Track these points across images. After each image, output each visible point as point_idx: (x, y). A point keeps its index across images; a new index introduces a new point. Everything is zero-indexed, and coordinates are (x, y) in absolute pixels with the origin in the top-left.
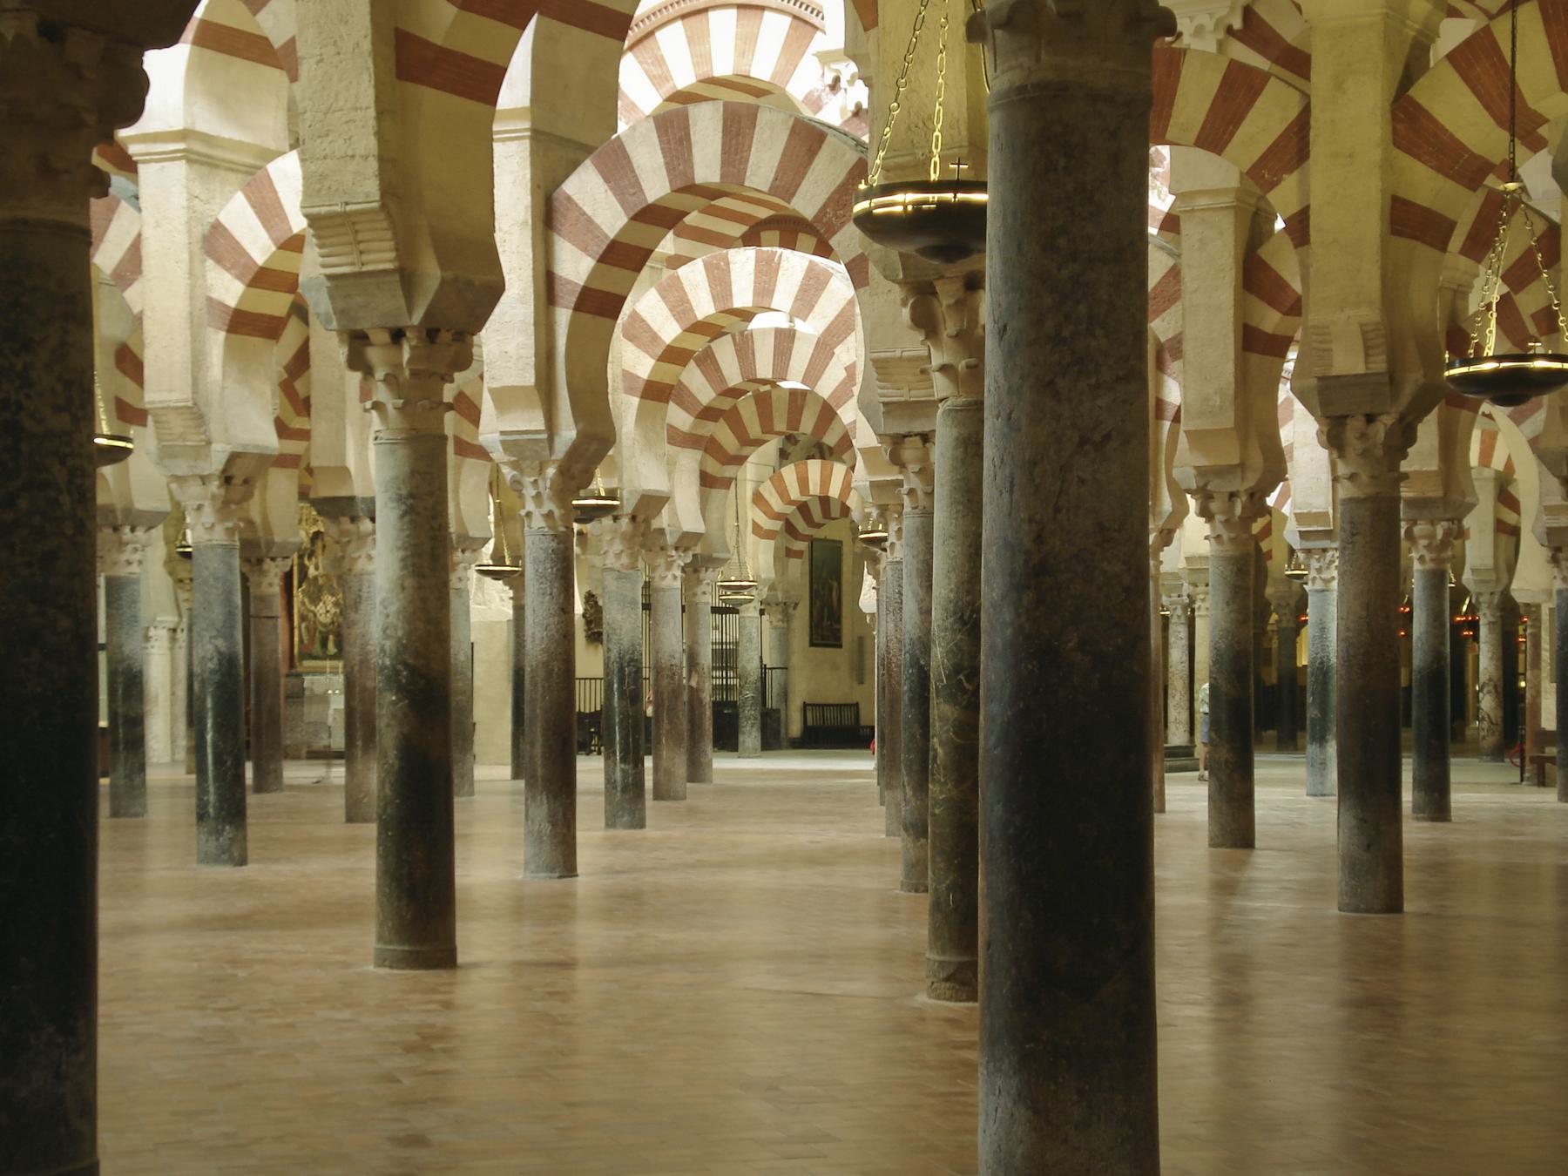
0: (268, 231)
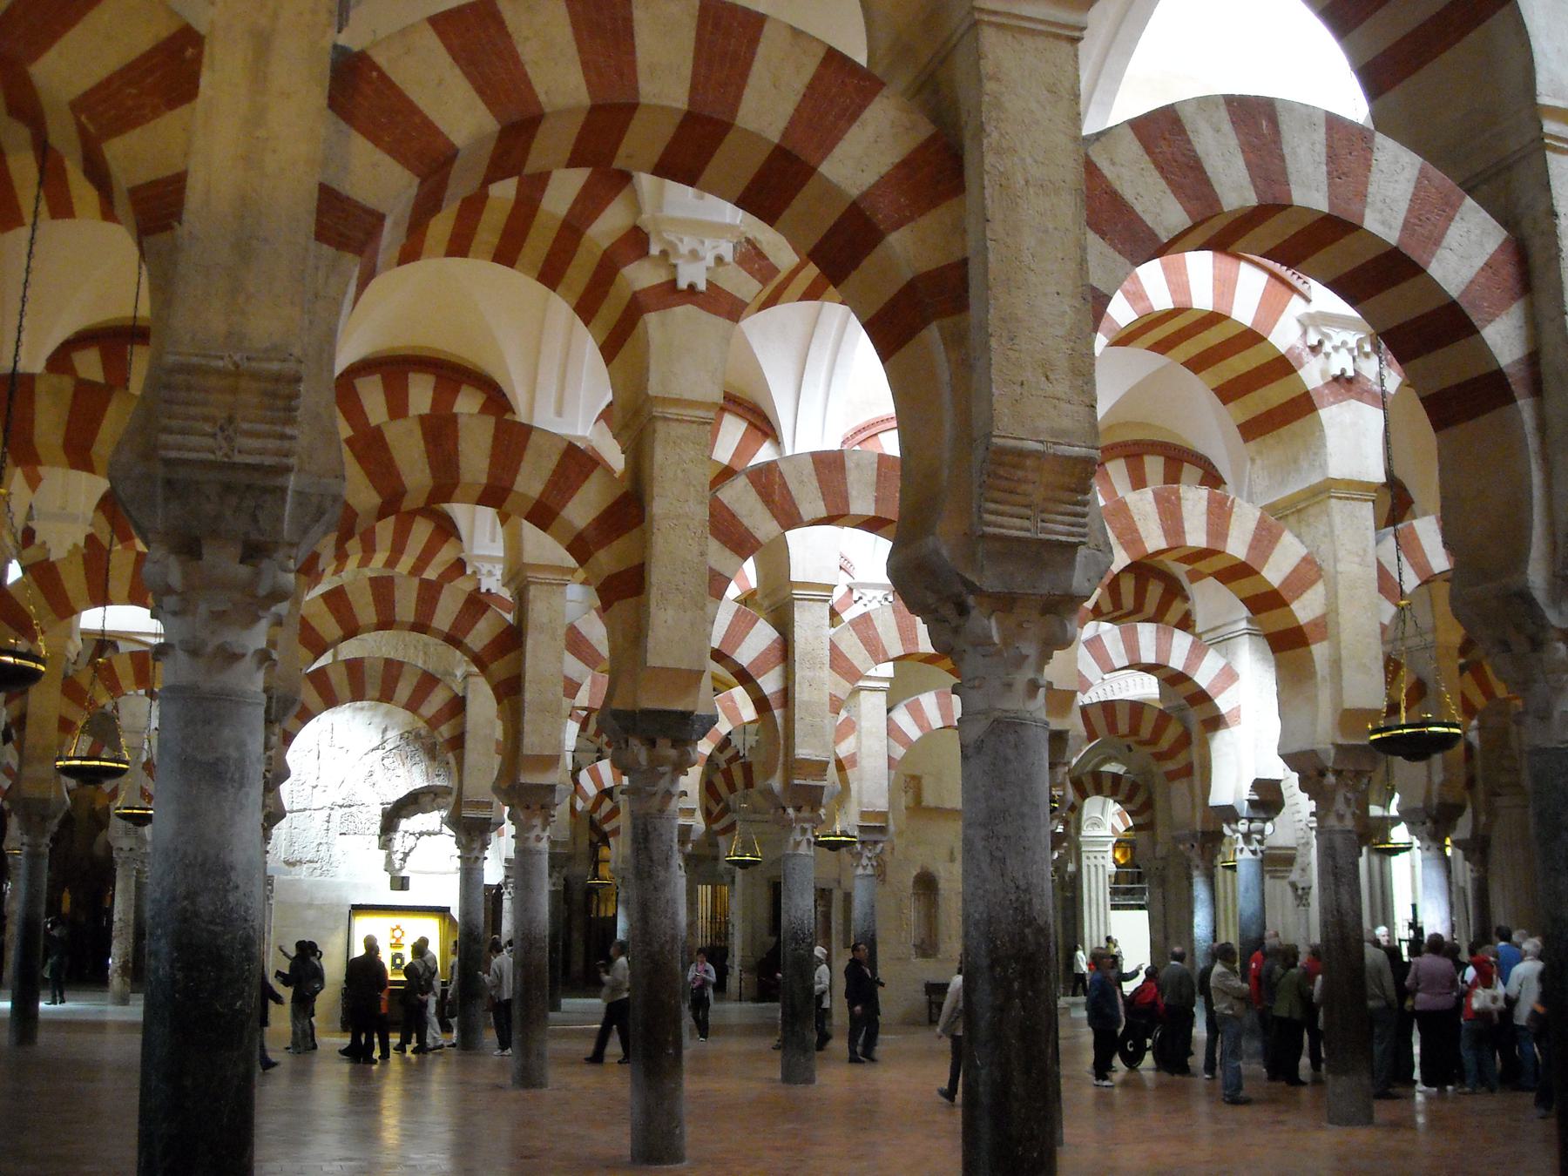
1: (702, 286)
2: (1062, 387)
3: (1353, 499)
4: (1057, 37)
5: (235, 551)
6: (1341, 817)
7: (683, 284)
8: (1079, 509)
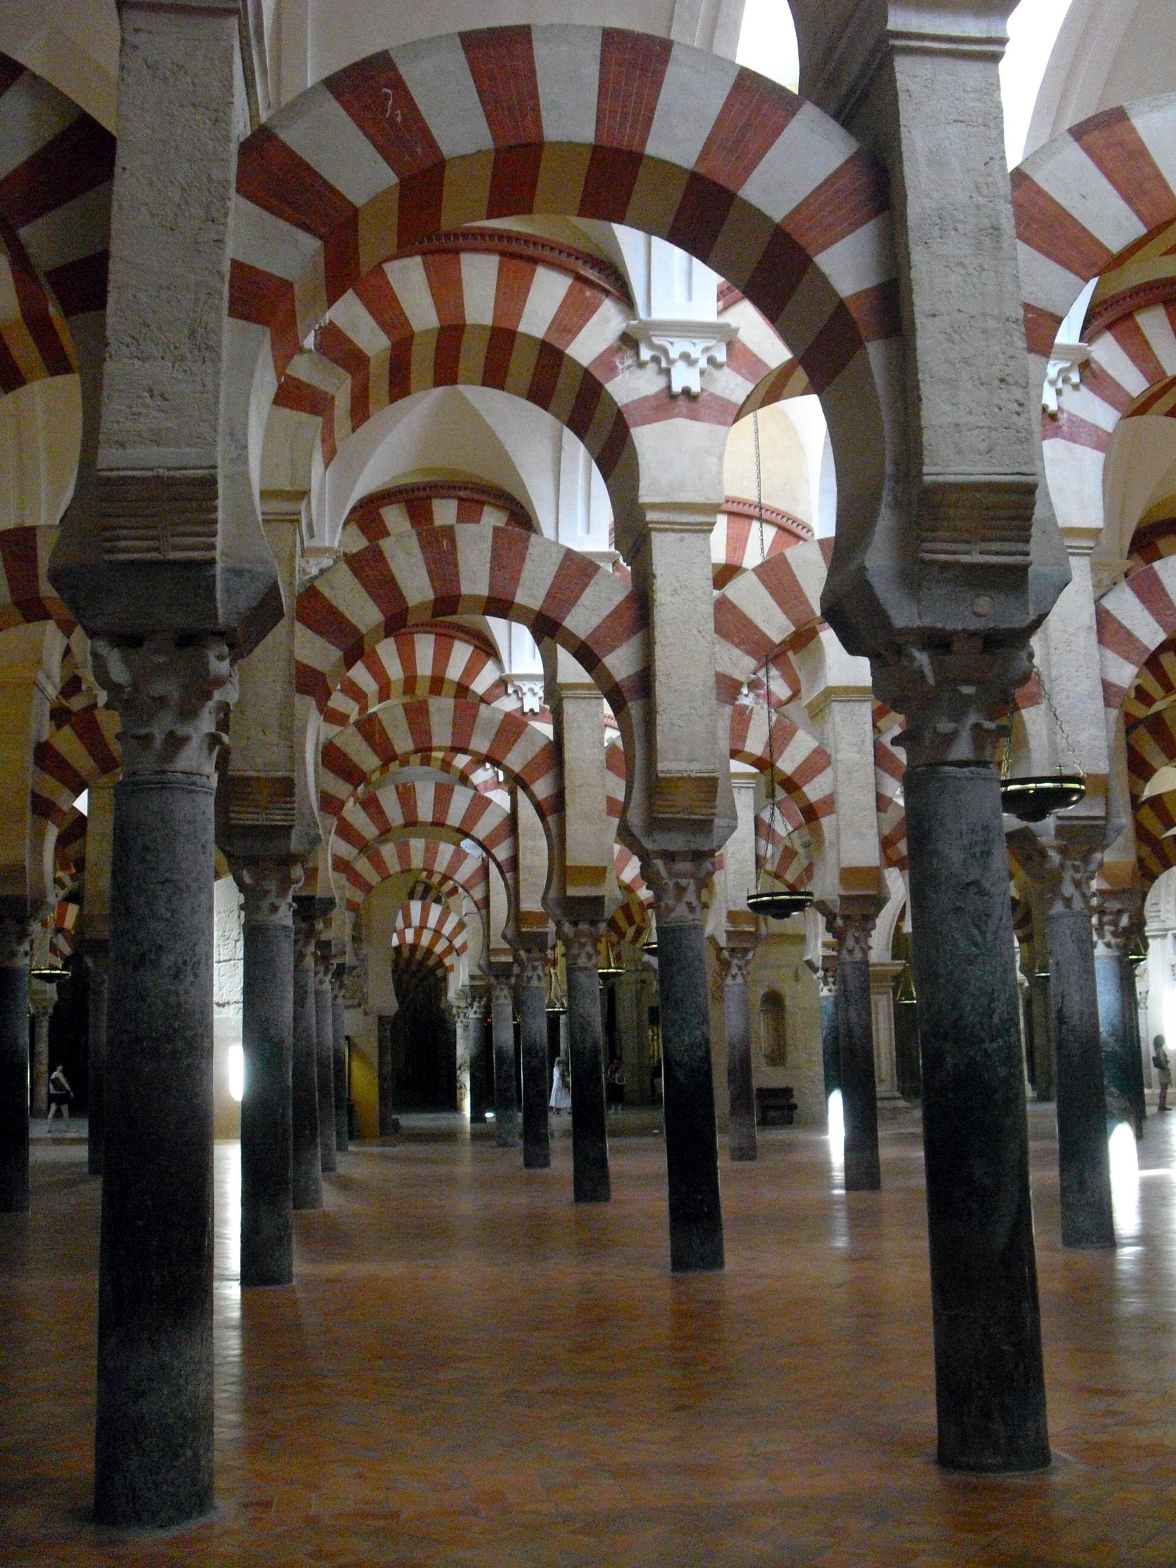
0: (785, 612)
2: (273, 738)
3: (853, 701)
4: (282, 521)
6: (851, 952)
8: (289, 806)
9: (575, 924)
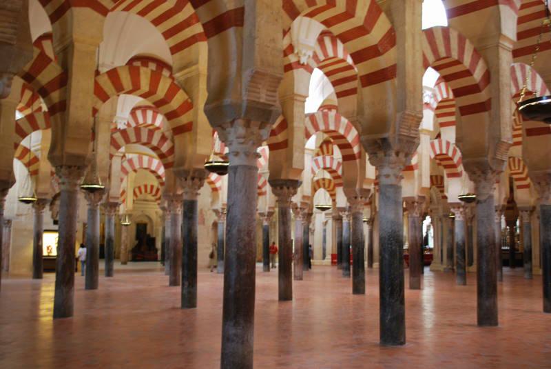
1: (306, 64)
5: (404, 155)
6: (416, 213)
7: (302, 62)
9: (361, 198)
